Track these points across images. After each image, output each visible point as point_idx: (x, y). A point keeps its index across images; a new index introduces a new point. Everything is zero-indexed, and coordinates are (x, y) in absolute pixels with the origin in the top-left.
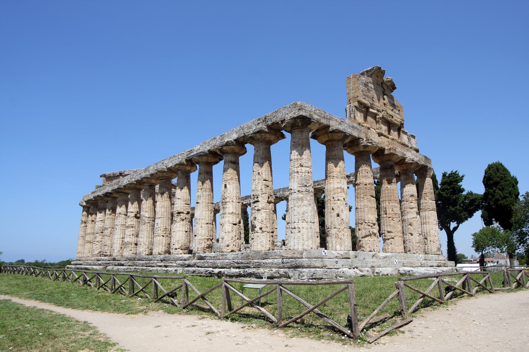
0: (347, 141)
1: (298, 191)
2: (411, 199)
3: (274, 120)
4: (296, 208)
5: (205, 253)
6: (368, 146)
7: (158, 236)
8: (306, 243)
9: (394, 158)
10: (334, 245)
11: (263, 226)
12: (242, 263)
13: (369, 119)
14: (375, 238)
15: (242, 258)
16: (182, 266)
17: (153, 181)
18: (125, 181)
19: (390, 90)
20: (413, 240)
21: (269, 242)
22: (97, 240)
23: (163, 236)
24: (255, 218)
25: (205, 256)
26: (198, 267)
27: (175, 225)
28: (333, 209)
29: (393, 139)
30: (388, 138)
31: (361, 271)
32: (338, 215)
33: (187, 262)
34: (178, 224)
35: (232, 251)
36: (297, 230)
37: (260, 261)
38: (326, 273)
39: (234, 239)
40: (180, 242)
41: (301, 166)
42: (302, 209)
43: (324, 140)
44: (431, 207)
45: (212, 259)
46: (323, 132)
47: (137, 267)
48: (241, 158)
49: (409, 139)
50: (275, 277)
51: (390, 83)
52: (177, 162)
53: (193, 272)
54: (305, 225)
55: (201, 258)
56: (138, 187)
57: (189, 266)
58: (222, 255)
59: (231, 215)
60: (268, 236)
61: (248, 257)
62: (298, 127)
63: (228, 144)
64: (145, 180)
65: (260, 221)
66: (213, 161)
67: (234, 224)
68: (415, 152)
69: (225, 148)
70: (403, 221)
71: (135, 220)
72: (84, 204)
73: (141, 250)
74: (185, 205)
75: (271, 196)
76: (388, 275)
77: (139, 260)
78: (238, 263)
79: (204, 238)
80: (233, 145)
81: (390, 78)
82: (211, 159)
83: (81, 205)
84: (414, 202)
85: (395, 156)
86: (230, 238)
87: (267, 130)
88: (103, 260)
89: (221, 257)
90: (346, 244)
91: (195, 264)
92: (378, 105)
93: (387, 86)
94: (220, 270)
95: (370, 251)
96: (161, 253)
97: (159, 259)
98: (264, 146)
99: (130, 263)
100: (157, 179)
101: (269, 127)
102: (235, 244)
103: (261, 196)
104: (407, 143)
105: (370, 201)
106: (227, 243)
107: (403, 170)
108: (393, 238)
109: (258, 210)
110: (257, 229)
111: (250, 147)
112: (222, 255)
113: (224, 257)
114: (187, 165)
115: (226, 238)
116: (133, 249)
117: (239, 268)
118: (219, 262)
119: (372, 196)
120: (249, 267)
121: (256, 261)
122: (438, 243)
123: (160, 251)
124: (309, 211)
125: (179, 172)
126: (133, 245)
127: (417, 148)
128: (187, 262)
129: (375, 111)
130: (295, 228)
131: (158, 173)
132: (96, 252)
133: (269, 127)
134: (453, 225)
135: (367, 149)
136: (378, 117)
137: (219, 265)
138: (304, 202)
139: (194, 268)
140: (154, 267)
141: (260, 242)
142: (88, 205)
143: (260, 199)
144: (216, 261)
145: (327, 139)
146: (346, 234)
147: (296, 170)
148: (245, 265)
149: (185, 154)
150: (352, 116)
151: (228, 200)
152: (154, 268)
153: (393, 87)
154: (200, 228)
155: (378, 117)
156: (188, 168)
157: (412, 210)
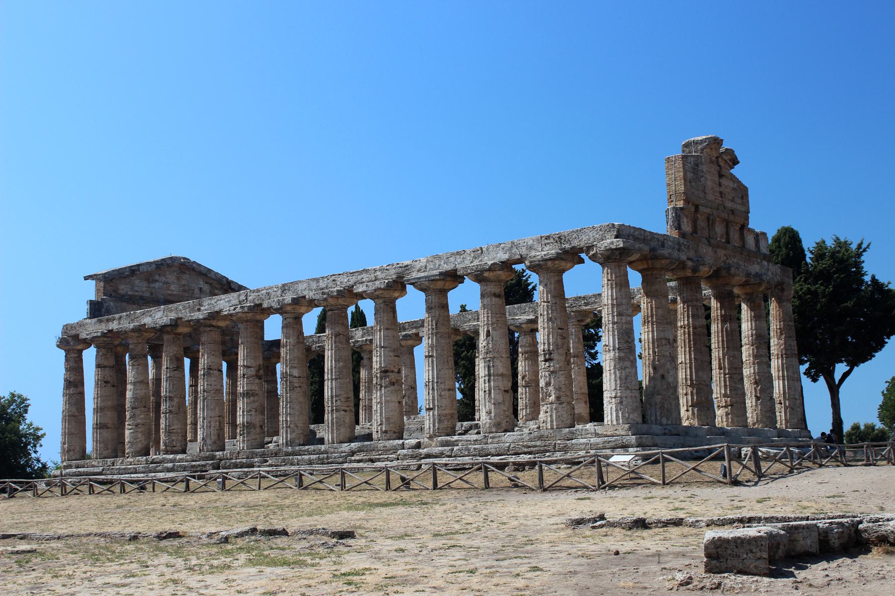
3: (575, 243)
8: (631, 416)
10: (659, 418)
18: (225, 303)
23: (346, 411)
30: (725, 249)
32: (663, 377)
40: (392, 421)
43: (641, 267)
57: (428, 456)
62: (615, 260)
64: (289, 308)
67: (505, 391)
69: (486, 274)
71: (257, 381)
78: (530, 447)
80: (502, 269)
89: (490, 440)
93: (726, 161)
101: (565, 252)
117: (530, 453)
118: (491, 447)
128: (423, 451)
131: (330, 300)
134: (840, 368)
137: (493, 451)
140: (342, 463)
142: (79, 347)
144: (485, 446)
145: (645, 266)
149: (392, 271)
153: (735, 162)
155: (711, 217)
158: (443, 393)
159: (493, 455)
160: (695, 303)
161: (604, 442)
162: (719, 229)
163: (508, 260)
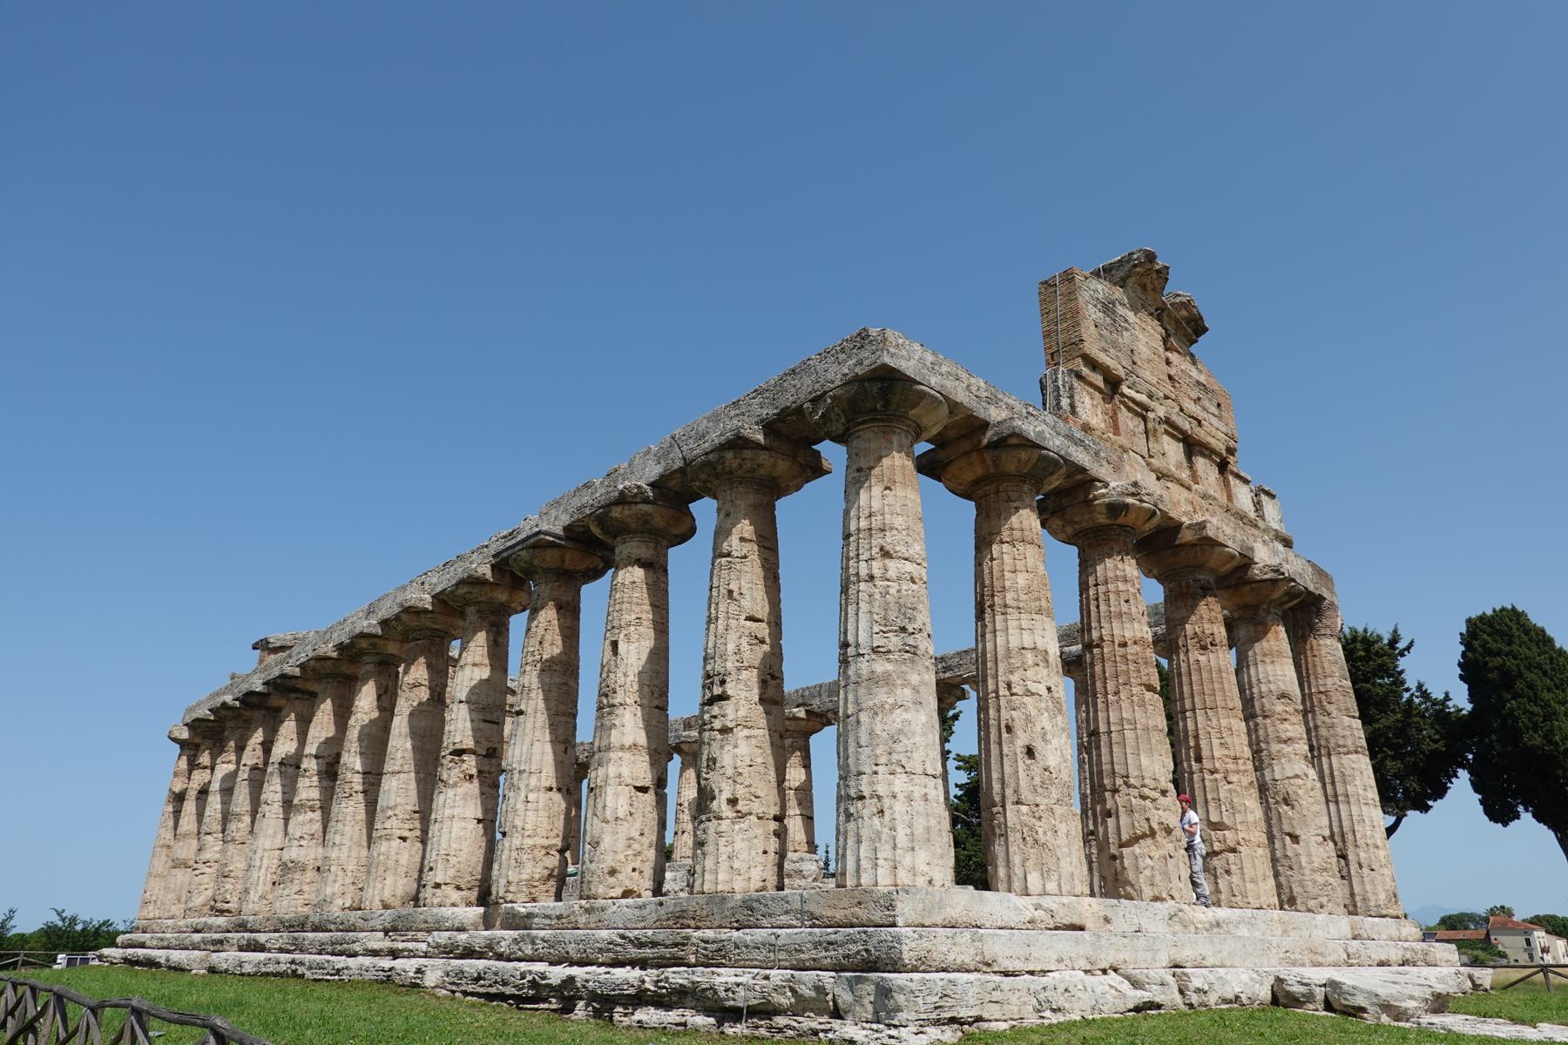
0: (1054, 482)
1: (875, 650)
2: (1279, 708)
4: (863, 717)
5: (534, 900)
6: (1127, 506)
7: (388, 838)
9: (1214, 560)
10: (1018, 870)
11: (741, 792)
12: (654, 944)
13: (1125, 417)
14: (1170, 847)
15: (659, 924)
16: (449, 951)
17: (392, 648)
19: (1186, 335)
20: (1304, 860)
21: (761, 858)
22: (206, 855)
23: (404, 839)
24: (713, 761)
25: (530, 916)
26: (499, 957)
27: (442, 797)
28: (1009, 729)
29: (1205, 496)
30: (1189, 489)
31: (1136, 984)
32: (1030, 752)
33: (462, 937)
34: (451, 793)
35: (627, 894)
36: (867, 809)
37: (725, 934)
38: (996, 995)
39: (636, 846)
40: (453, 860)
41: (886, 554)
42: (888, 719)
43: (969, 476)
44: (1349, 742)
45: (551, 927)
46: (966, 445)
47: (298, 956)
48: (675, 555)
49: (1258, 506)
50: (777, 1011)
51: (1184, 313)
52: (459, 572)
53: (479, 978)
54: (900, 783)
55: (518, 922)
56: (347, 669)
57: (469, 953)
58: (588, 911)
59: (627, 756)
60: (759, 832)
61: (680, 918)
63: (623, 499)
64: (364, 644)
65: (729, 772)
66: (582, 567)
68: (1280, 547)
69: (616, 512)
70: (1263, 789)
72: (185, 735)
73: (329, 891)
74: (482, 725)
75: (773, 677)
76: (1237, 997)
77: (316, 929)
78: (641, 945)
79: (529, 842)
80: (646, 501)
81: (1185, 294)
82: (573, 560)
83: (174, 740)
84: (1293, 719)
85: (1218, 549)
86: (621, 844)
87: (760, 437)
88: (210, 929)
90: (1065, 867)
91: (490, 947)
92: (1152, 373)
93: (1177, 322)
94: (575, 971)
95: (1156, 899)
96: (391, 901)
97: (376, 923)
98: (751, 499)
99: (283, 938)
100: (405, 638)
102: (637, 865)
103: (734, 677)
104: (1252, 515)
105: (1142, 704)
106: (609, 862)
107: (1246, 607)
108: (1234, 850)
109: (725, 730)
110: (720, 804)
111: (704, 511)
112: (588, 911)
113: (594, 918)
114: (495, 585)
115: (606, 842)
116: (306, 888)
117: (643, 964)
119: (1150, 688)
120: (679, 962)
121: (709, 934)
122: (1386, 871)
123: (387, 895)
124: (919, 730)
125: (471, 611)
126: (310, 875)
127: (1284, 531)
128: (462, 937)
129: (1143, 398)
130: (862, 798)
131: (405, 617)
132: (198, 901)
133: (768, 426)
135: (1121, 520)
136: (1151, 415)
137: (572, 950)
138: (898, 691)
139: (481, 964)
140: (355, 955)
141: (738, 860)
142: (197, 740)
143: (730, 689)
145: (979, 471)
146: (1062, 828)
147: (863, 572)
148: (667, 952)
150: (1065, 402)
151: (617, 700)
152: (351, 962)
154: (520, 806)
155: (1151, 415)
156: (502, 596)
157: (1287, 749)
158: (531, 797)
159: (572, 964)
160: (1122, 587)
161: (817, 945)
162: (1173, 451)
163: (662, 476)
